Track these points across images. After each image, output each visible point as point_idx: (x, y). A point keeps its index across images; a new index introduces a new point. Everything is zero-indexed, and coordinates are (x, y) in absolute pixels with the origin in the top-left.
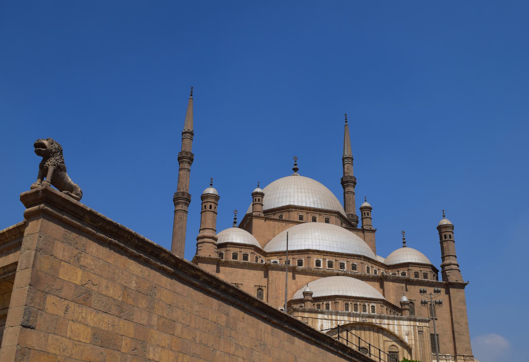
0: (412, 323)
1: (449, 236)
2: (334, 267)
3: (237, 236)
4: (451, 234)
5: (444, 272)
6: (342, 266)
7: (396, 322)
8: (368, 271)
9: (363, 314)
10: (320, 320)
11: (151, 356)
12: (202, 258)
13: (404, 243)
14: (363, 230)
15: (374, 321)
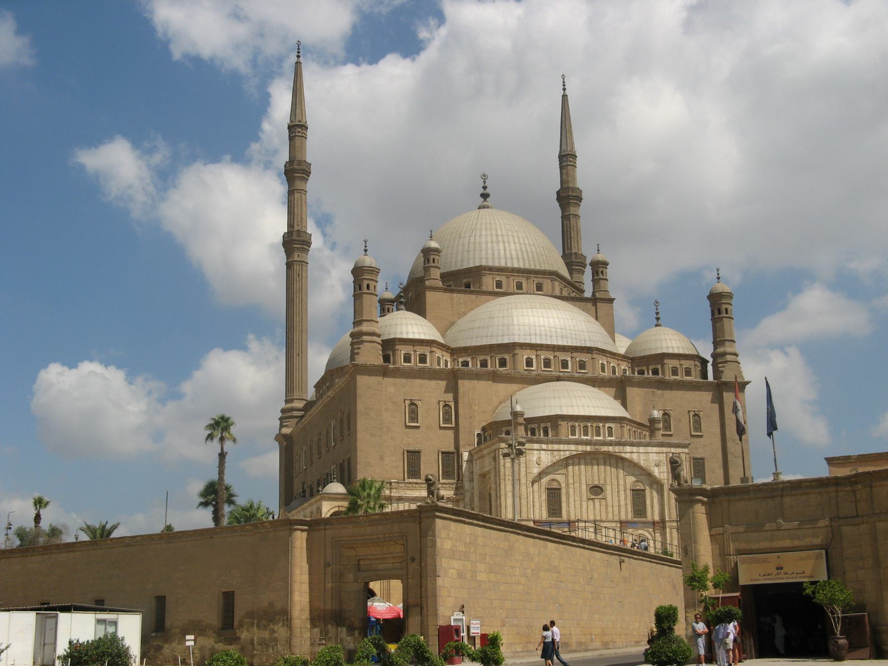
0: (665, 449)
1: (724, 311)
2: (553, 366)
3: (408, 326)
4: (727, 306)
5: (715, 365)
6: (565, 364)
7: (642, 449)
8: (603, 370)
9: (597, 440)
10: (535, 452)
11: (478, 578)
12: (362, 365)
13: (658, 319)
14: (594, 300)
15: (611, 449)
